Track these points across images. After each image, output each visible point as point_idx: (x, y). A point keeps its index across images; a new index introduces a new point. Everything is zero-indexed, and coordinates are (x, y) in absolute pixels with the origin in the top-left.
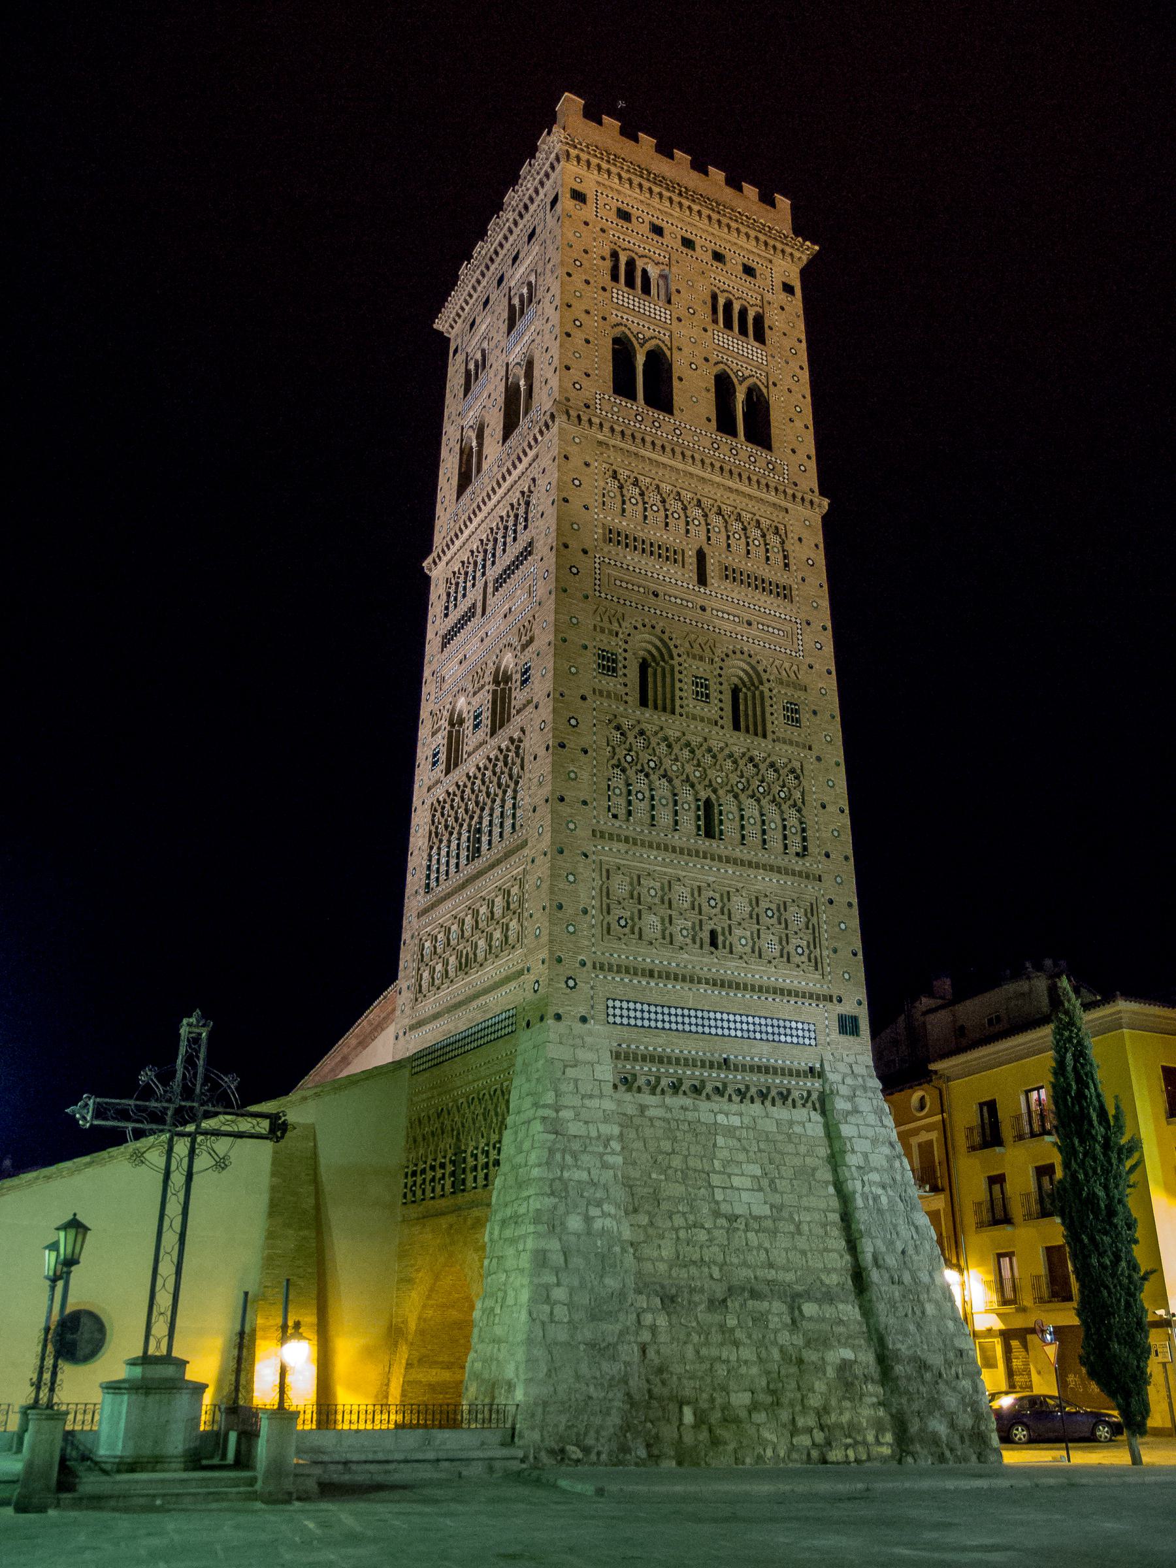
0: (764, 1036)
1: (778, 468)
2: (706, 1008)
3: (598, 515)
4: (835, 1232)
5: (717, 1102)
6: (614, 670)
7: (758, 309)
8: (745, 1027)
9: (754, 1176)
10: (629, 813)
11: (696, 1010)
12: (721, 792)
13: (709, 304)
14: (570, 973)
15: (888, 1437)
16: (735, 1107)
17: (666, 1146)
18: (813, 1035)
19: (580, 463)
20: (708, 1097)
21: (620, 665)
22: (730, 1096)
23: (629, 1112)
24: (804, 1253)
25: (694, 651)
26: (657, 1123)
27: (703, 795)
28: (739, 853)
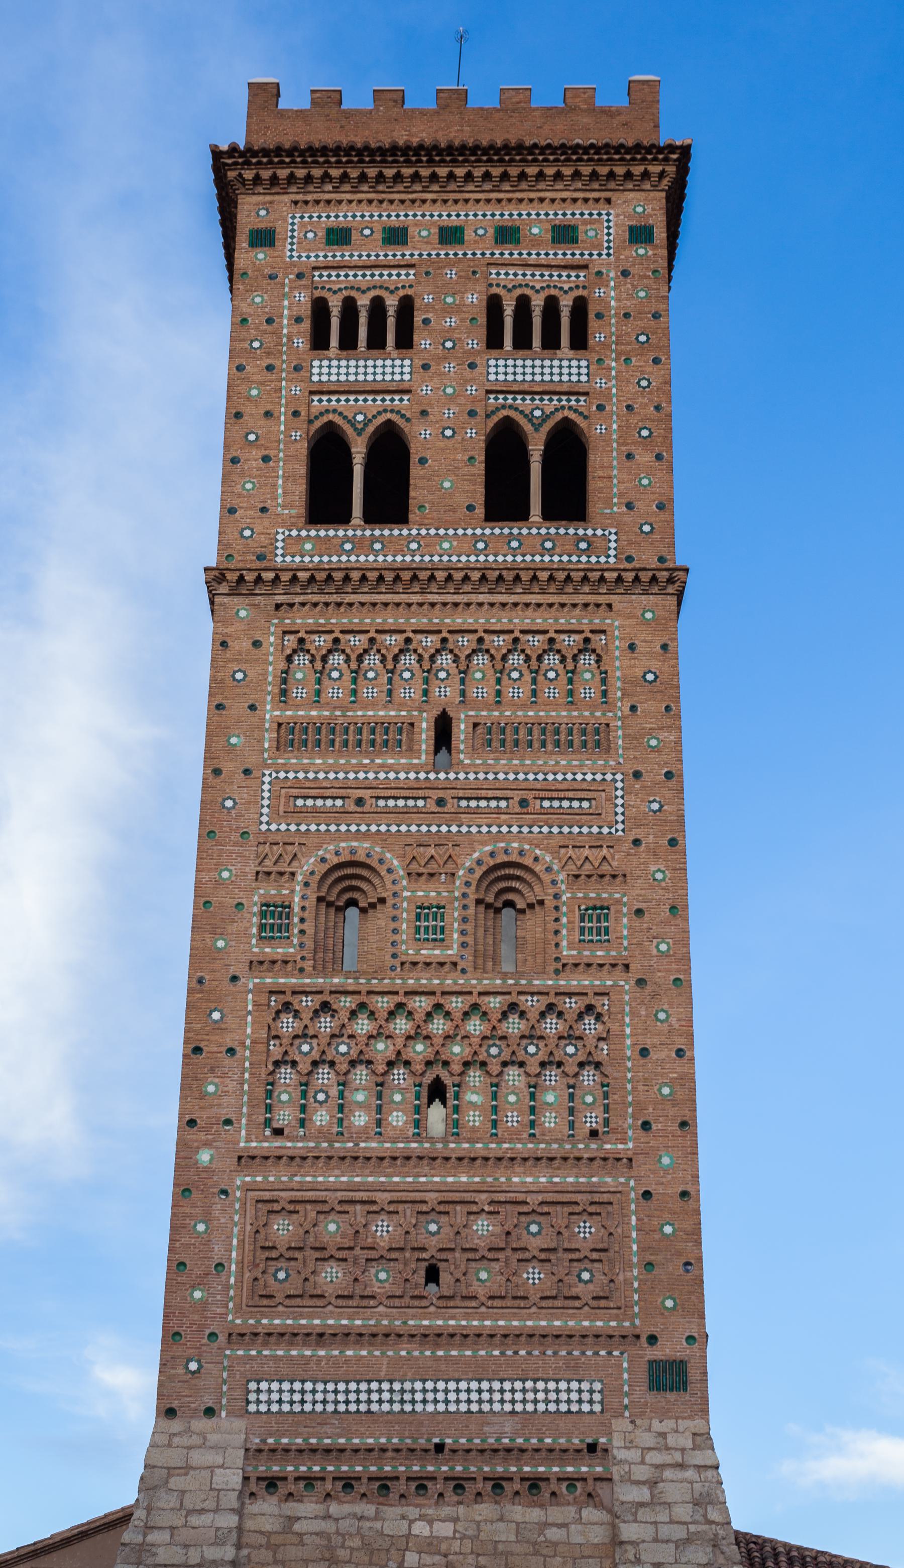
1: (598, 543)
3: (271, 713)
5: (416, 1506)
7: (580, 292)
10: (302, 1123)
11: (391, 1382)
13: (482, 320)
16: (446, 1511)
19: (247, 644)
22: (441, 1495)
23: (268, 1527)
25: (422, 870)
26: (307, 1539)
27: (428, 1079)
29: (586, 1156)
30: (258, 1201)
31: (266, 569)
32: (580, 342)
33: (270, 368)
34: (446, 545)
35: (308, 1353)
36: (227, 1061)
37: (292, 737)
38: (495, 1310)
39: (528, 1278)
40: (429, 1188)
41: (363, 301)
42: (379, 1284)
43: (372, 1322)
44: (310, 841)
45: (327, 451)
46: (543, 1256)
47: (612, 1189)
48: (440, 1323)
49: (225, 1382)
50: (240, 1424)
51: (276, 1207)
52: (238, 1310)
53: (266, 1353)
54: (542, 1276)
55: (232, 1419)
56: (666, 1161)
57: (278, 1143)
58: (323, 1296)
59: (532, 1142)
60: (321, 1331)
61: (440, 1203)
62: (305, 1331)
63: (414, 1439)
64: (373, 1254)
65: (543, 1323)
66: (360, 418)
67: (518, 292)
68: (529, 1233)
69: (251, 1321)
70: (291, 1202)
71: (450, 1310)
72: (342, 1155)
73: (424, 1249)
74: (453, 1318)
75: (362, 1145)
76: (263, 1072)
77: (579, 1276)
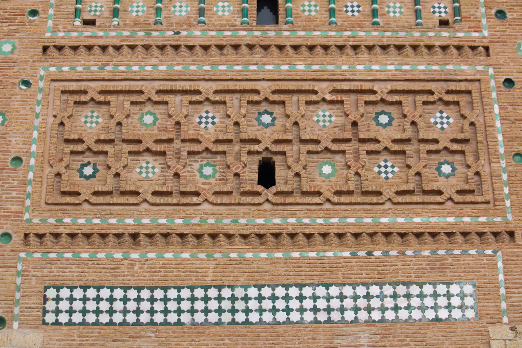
2: (242, 281)
10: (115, 12)
11: (220, 288)
28: (317, 36)
29: (437, 44)
30: (63, 92)
35: (118, 255)
38: (343, 207)
39: (380, 173)
40: (261, 77)
42: (203, 180)
43: (196, 221)
46: (396, 147)
47: (469, 78)
48: (277, 221)
49: (18, 289)
51: (83, 98)
52: (35, 208)
53: (68, 255)
54: (396, 169)
55: (26, 331)
57: (89, 31)
58: (136, 193)
59: (375, 30)
60: (133, 231)
61: (274, 92)
62: (116, 232)
64: (195, 147)
65: (401, 220)
68: (378, 124)
69: (52, 221)
70: (101, 92)
71: (289, 208)
72: (160, 43)
73: (257, 141)
74: (293, 215)
75: (184, 33)
77: (438, 169)
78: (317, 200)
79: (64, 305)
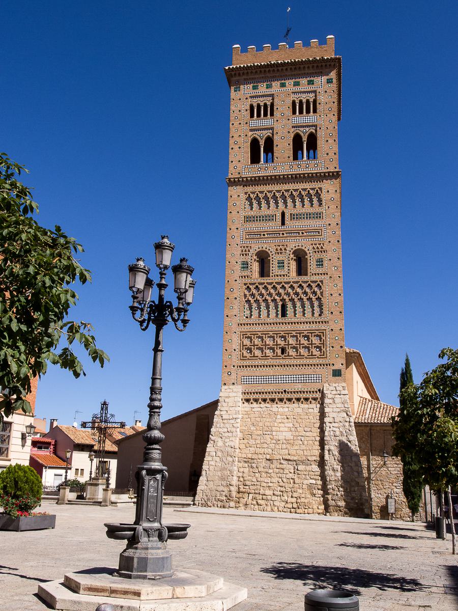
0: (300, 381)
3: (243, 214)
4: (318, 443)
6: (247, 267)
8: (292, 379)
9: (289, 427)
11: (274, 376)
12: (287, 300)
13: (291, 107)
14: (229, 370)
15: (322, 507)
16: (286, 405)
17: (258, 419)
18: (320, 378)
20: (277, 403)
21: (249, 265)
23: (247, 410)
24: (303, 450)
28: (293, 320)
31: (240, 178)
32: (315, 111)
33: (240, 124)
34: (283, 168)
36: (235, 301)
37: (248, 219)
41: (262, 104)
44: (253, 246)
45: (255, 143)
46: (308, 345)
50: (240, 387)
56: (336, 321)
63: (279, 389)
66: (262, 135)
67: (299, 99)
76: (243, 303)
78: (293, 357)
79: (245, 380)
